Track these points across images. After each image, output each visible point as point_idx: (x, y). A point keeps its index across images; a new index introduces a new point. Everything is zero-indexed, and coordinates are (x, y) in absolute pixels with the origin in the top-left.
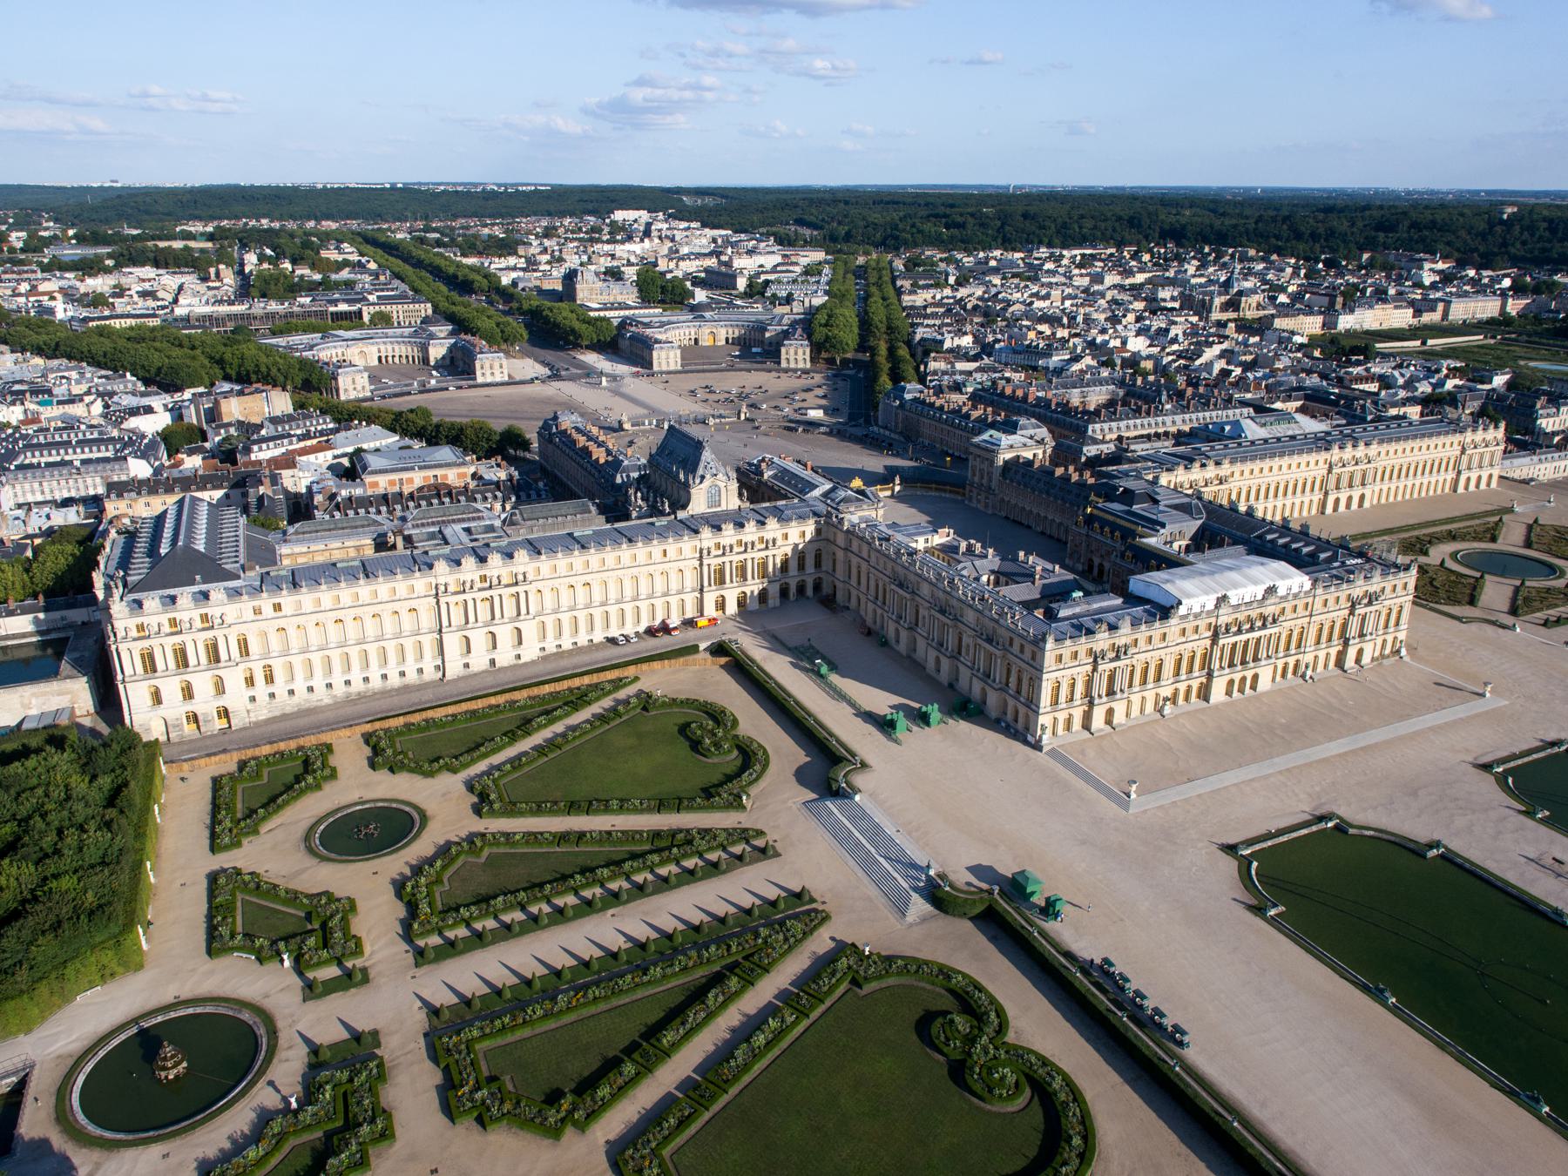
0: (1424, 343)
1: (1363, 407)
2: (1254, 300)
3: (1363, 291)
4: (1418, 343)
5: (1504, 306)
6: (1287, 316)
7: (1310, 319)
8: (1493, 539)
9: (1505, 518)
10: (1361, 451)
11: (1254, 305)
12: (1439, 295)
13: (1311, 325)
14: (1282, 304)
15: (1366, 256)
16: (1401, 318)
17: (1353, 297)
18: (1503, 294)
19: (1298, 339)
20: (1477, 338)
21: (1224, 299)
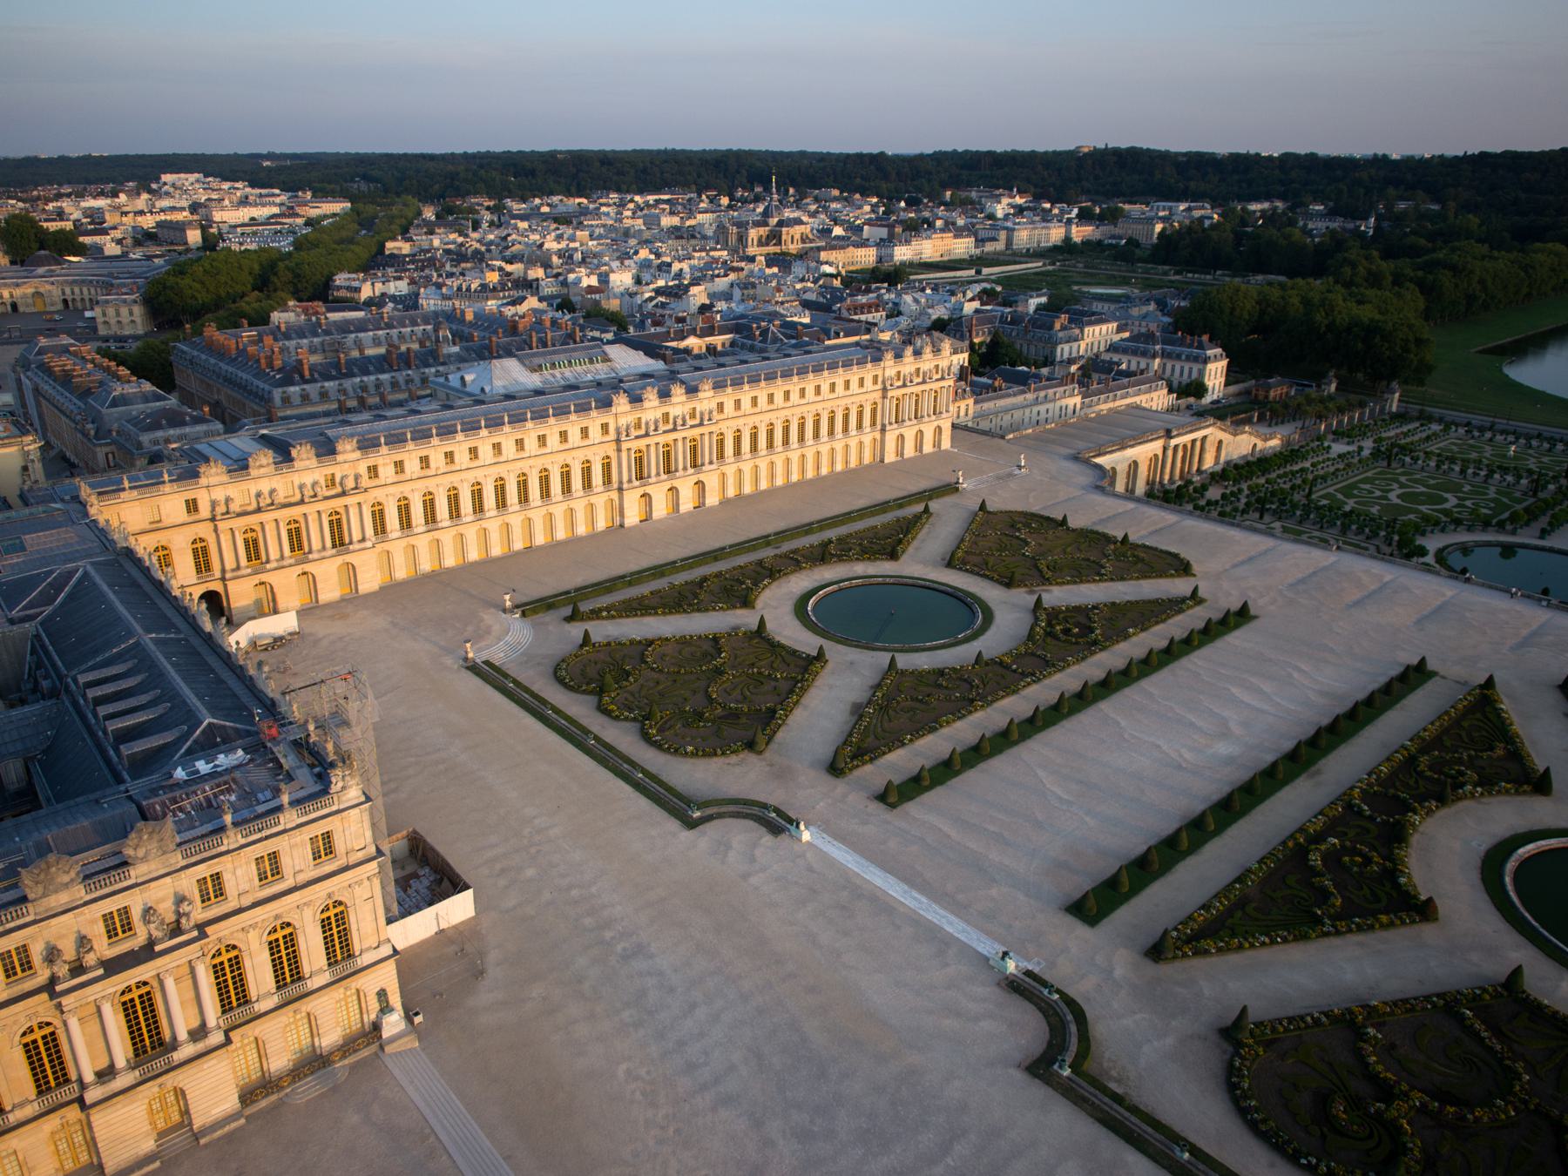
0: (978, 272)
1: (765, 332)
2: (797, 231)
3: (931, 225)
4: (972, 272)
5: (1068, 232)
6: (833, 248)
7: (861, 252)
8: (893, 556)
9: (934, 505)
10: (679, 403)
11: (797, 237)
12: (1009, 224)
13: (866, 257)
14: (837, 238)
15: (948, 193)
16: (962, 247)
17: (914, 229)
18: (1069, 221)
19: (827, 269)
20: (1035, 265)
21: (763, 231)
